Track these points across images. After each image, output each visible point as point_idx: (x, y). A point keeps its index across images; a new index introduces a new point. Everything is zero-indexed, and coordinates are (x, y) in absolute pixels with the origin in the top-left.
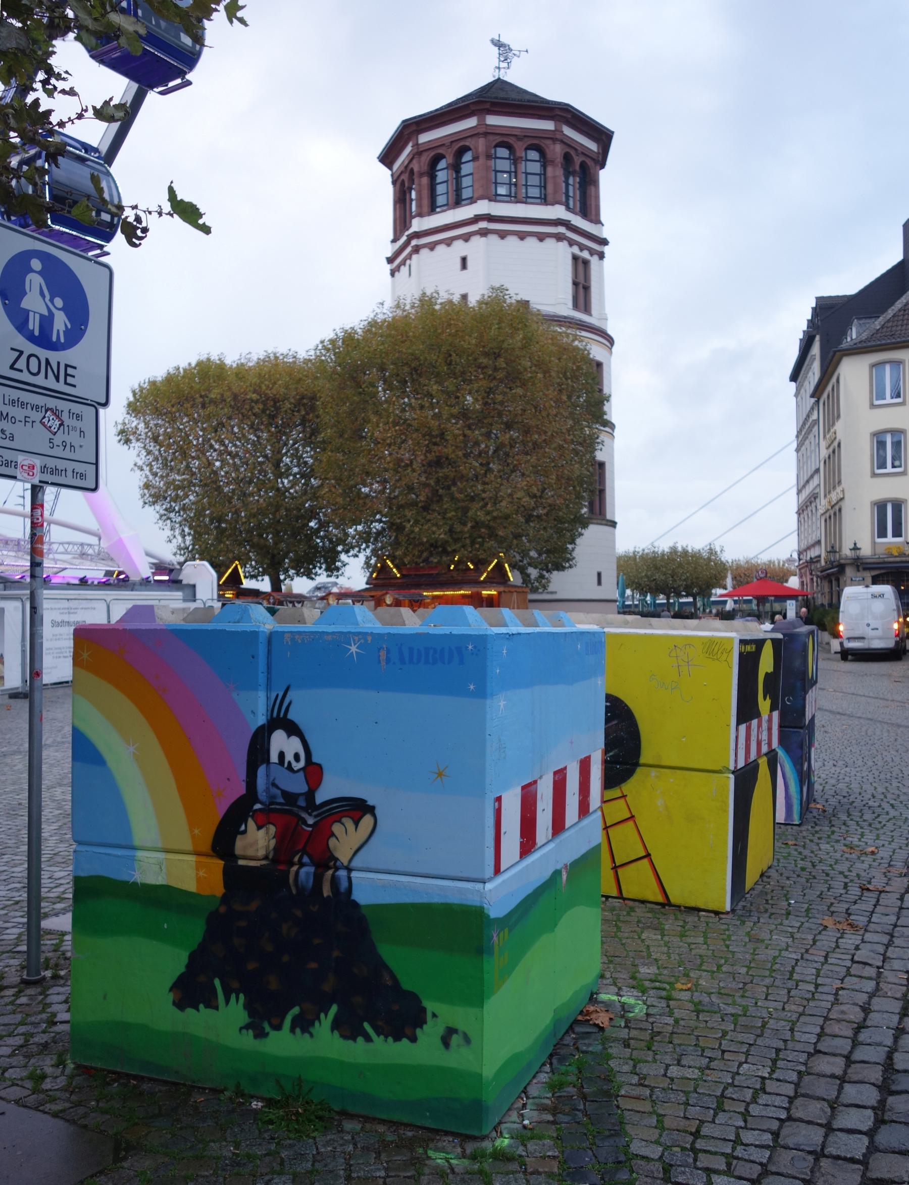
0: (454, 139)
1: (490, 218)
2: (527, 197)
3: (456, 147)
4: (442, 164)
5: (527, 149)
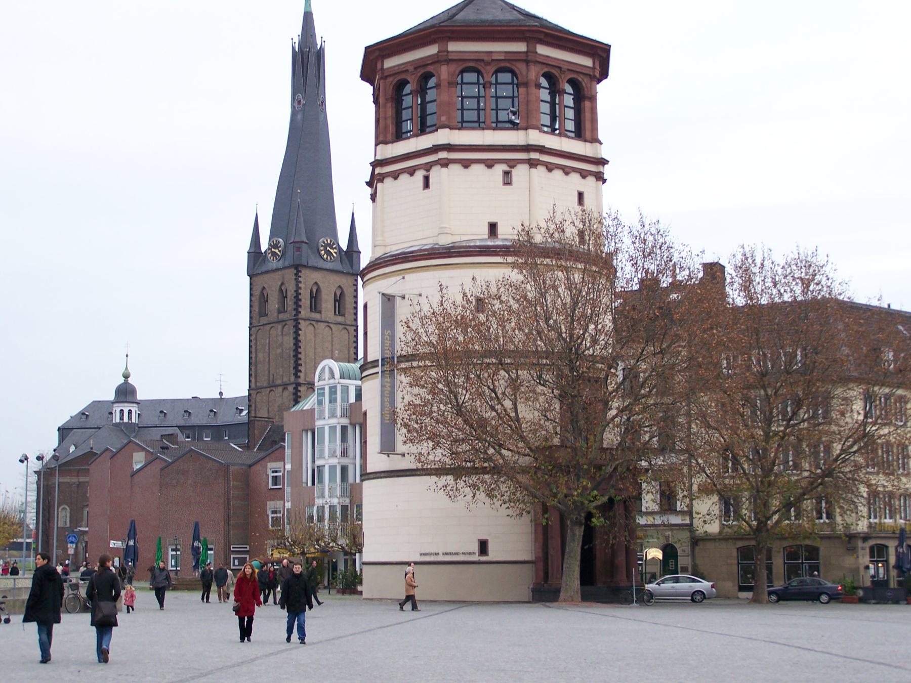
0: (419, 64)
1: (449, 148)
2: (497, 122)
3: (421, 72)
4: (408, 89)
5: (496, 72)
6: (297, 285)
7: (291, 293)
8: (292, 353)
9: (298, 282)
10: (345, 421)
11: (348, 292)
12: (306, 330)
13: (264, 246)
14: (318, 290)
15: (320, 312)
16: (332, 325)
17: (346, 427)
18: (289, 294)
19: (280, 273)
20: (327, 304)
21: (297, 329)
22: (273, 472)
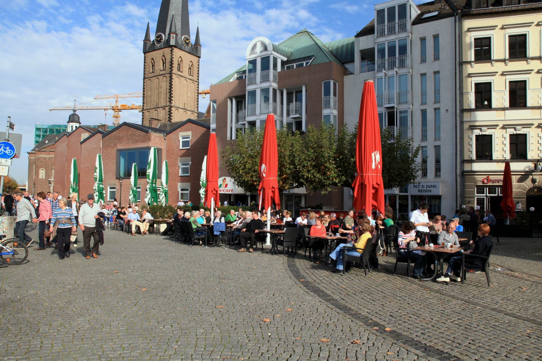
6: (172, 56)
8: (168, 91)
9: (172, 55)
10: (275, 85)
11: (195, 65)
12: (176, 80)
13: (153, 37)
14: (181, 61)
18: (167, 61)
19: (162, 50)
22: (183, 138)
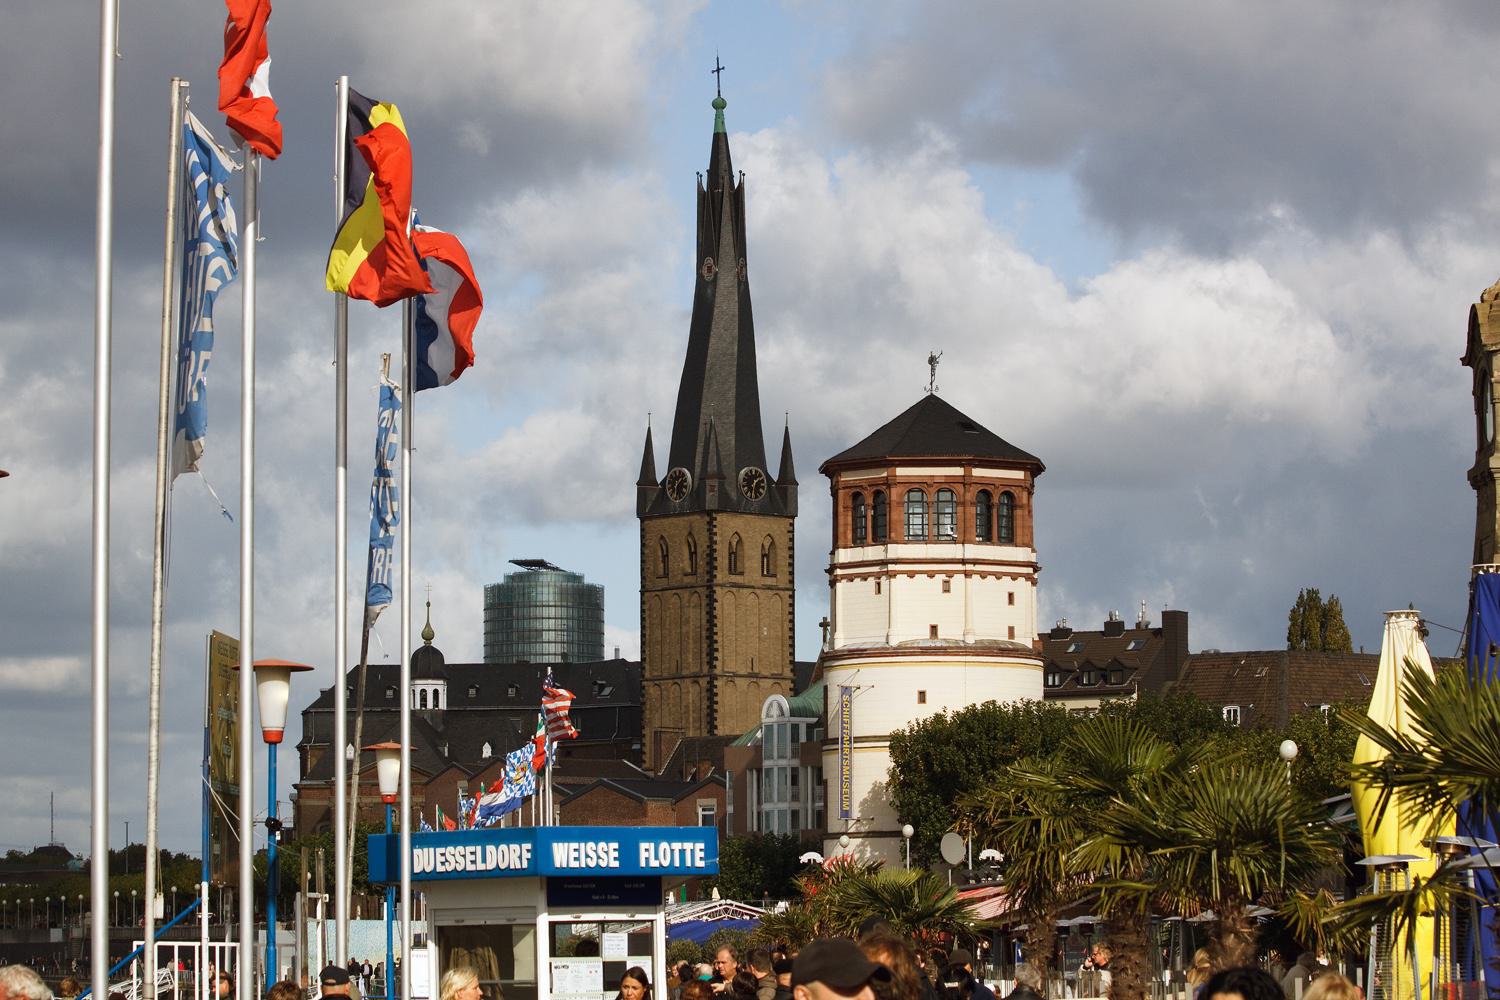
6: (711, 539)
7: (702, 549)
9: (712, 534)
10: (796, 763)
11: (782, 542)
12: (725, 601)
13: (661, 471)
14: (740, 541)
15: (742, 574)
16: (758, 591)
17: (797, 768)
18: (699, 550)
20: (752, 562)
21: (711, 600)
